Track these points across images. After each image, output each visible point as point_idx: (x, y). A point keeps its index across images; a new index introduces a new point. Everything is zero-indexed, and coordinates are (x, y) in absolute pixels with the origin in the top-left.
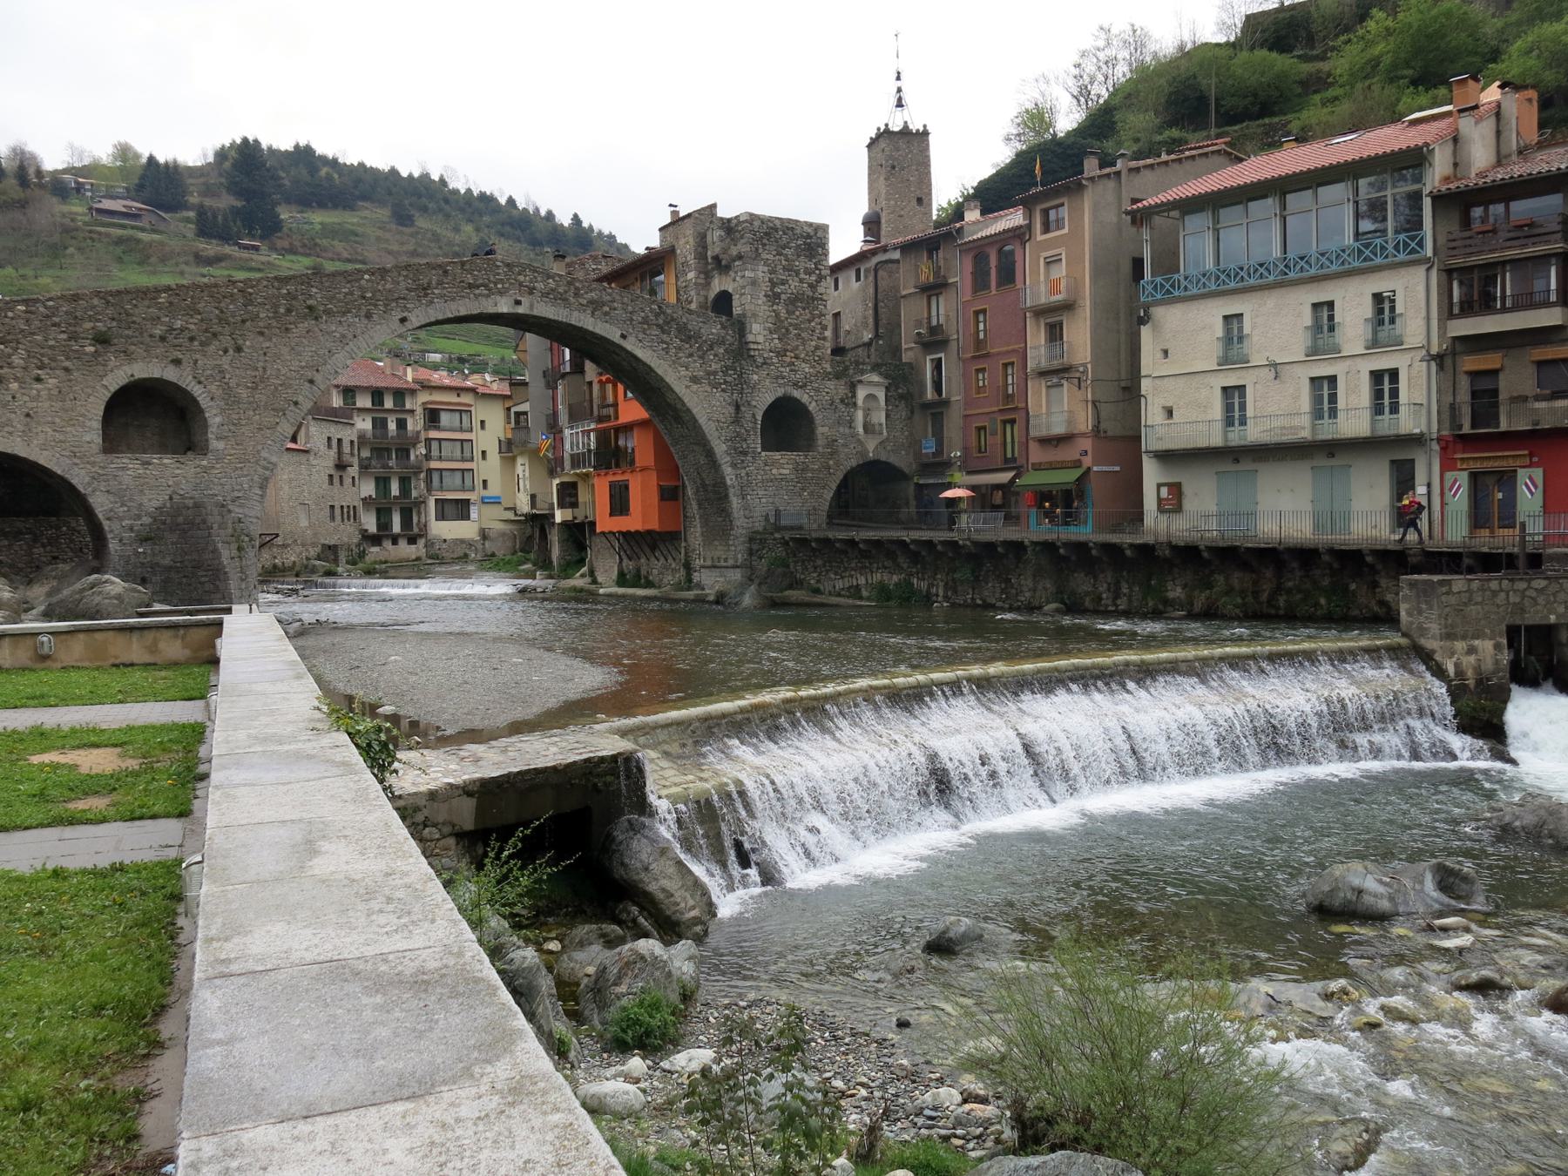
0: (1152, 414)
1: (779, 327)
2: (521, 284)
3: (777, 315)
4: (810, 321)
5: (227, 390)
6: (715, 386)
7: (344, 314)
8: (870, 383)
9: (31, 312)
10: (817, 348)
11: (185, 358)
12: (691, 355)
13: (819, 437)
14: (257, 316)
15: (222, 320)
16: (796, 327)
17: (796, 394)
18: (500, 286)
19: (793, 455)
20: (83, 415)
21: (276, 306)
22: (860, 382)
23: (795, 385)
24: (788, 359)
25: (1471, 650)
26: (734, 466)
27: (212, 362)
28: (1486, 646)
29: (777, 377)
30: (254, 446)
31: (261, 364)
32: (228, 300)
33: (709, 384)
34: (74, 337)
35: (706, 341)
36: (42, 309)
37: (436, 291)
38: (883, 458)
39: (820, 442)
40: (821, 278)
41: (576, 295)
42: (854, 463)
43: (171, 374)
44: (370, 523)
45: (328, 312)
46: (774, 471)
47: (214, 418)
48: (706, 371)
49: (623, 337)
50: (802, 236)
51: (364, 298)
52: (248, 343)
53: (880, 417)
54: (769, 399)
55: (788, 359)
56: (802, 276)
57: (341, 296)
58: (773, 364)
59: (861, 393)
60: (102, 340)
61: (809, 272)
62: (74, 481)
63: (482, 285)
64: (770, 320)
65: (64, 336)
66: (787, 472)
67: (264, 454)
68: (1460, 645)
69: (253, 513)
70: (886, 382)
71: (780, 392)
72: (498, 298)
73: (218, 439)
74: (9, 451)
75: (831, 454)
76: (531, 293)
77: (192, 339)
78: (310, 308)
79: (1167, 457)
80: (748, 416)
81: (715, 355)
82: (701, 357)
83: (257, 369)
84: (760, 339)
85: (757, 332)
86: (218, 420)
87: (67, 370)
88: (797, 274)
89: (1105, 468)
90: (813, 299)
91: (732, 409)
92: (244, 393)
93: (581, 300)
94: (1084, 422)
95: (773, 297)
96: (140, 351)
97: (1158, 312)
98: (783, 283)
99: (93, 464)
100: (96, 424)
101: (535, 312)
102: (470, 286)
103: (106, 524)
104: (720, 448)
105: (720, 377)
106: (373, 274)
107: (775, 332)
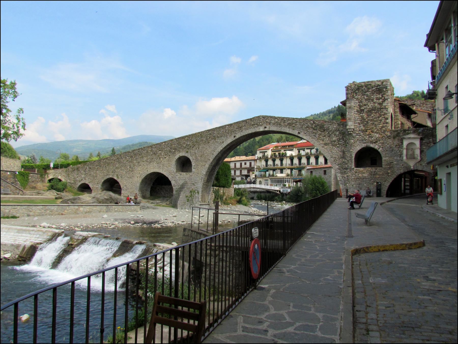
2: (267, 122)
3: (362, 117)
4: (379, 117)
5: (196, 157)
7: (221, 137)
8: (409, 138)
10: (382, 127)
11: (189, 151)
12: (325, 136)
13: (383, 161)
15: (196, 142)
16: (371, 120)
17: (372, 146)
19: (369, 169)
22: (404, 138)
23: (372, 142)
24: (367, 133)
26: (341, 173)
27: (193, 151)
29: (362, 140)
33: (332, 145)
35: (331, 131)
39: (383, 164)
40: (385, 100)
41: (284, 122)
42: (402, 171)
43: (186, 155)
45: (218, 137)
46: (359, 175)
47: (193, 164)
49: (299, 133)
50: (374, 85)
51: (226, 132)
53: (418, 152)
54: (358, 148)
55: (367, 133)
56: (374, 101)
58: (361, 135)
59: (405, 143)
61: (378, 99)
62: (169, 178)
64: (358, 120)
66: (367, 175)
67: (202, 172)
69: (200, 186)
71: (364, 145)
72: (260, 127)
73: (194, 169)
74: (160, 172)
75: (390, 168)
76: (270, 124)
77: (190, 147)
78: (214, 136)
80: (349, 156)
81: (335, 135)
82: (329, 136)
84: (353, 127)
85: (351, 125)
86: (194, 164)
87: (169, 155)
88: (372, 100)
90: (381, 109)
91: (341, 153)
92: (199, 158)
95: (361, 111)
96: (181, 150)
98: (365, 105)
99: (172, 174)
101: (271, 129)
102: (253, 125)
103: (173, 187)
107: (362, 124)
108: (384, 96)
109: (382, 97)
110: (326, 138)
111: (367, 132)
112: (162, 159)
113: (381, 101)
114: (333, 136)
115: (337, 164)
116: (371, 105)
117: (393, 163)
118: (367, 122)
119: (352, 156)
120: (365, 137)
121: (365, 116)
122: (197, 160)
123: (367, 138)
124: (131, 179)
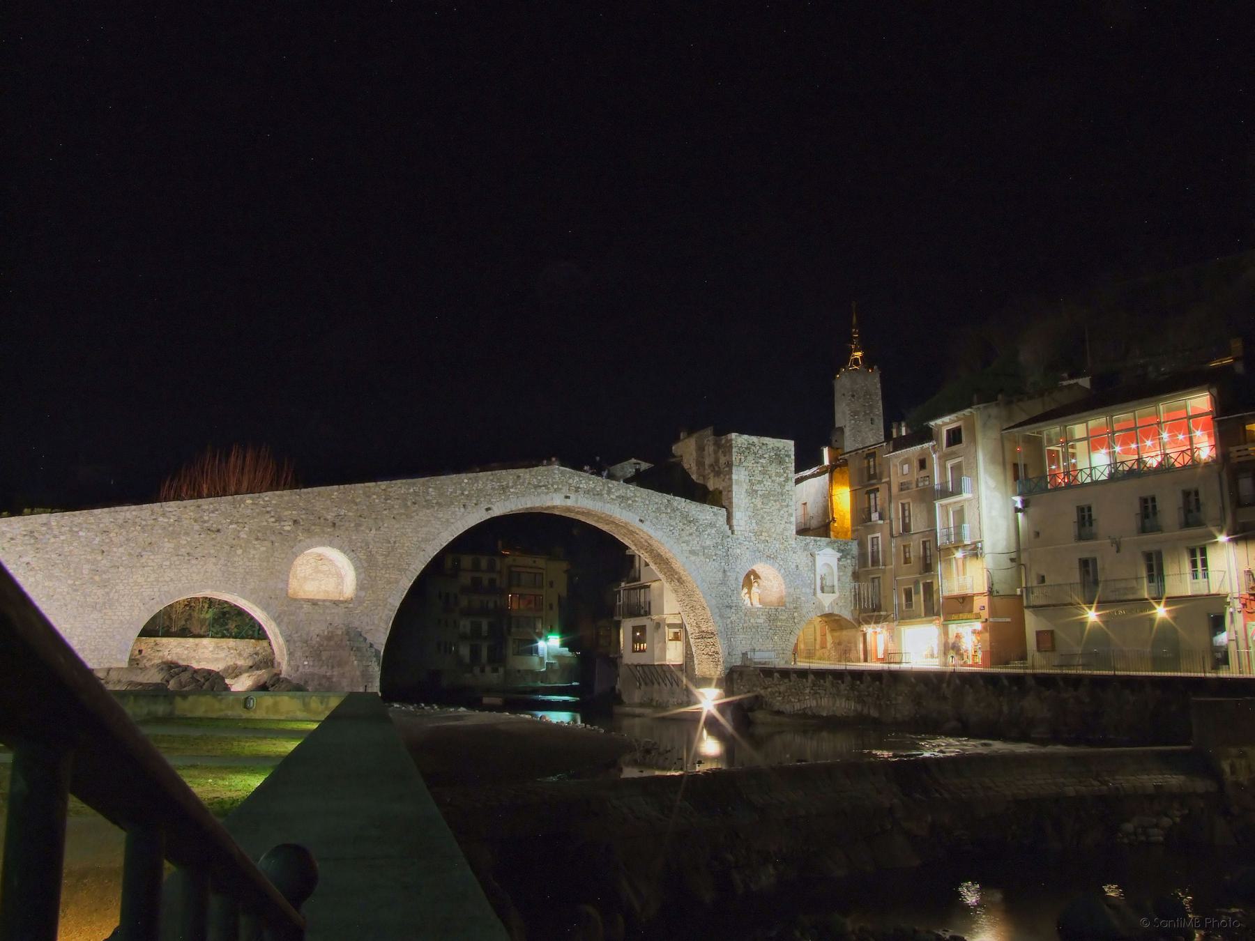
4: (779, 510)
6: (709, 557)
9: (255, 504)
10: (785, 529)
12: (691, 534)
14: (393, 507)
18: (555, 486)
20: (279, 572)
21: (405, 500)
30: (384, 595)
31: (393, 539)
32: (375, 497)
34: (279, 520)
35: (701, 525)
36: (261, 502)
37: (512, 490)
38: (836, 612)
48: (701, 546)
52: (386, 525)
55: (763, 538)
57: (449, 493)
60: (295, 522)
63: (543, 486)
65: (273, 520)
66: (762, 621)
67: (390, 600)
68: (1233, 751)
70: (839, 555)
75: (795, 608)
82: (697, 536)
83: (389, 542)
89: (1000, 620)
91: (720, 575)
92: (380, 559)
93: (612, 496)
96: (317, 529)
98: (760, 482)
105: (712, 551)
106: (470, 479)
108: (787, 471)
109: (785, 472)
110: (693, 540)
111: (761, 535)
112: (239, 552)
113: (782, 479)
114: (706, 536)
115: (713, 595)
117: (800, 598)
118: (763, 517)
119: (738, 581)
120: (759, 545)
121: (758, 502)
123: (761, 547)
124: (95, 615)
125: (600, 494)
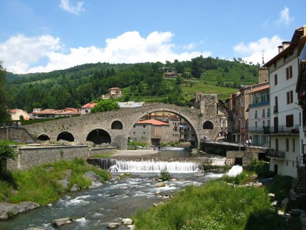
0: (249, 126)
1: (207, 110)
17: (210, 120)
25: (230, 160)
28: (232, 160)
40: (215, 102)
43: (119, 120)
44: (183, 137)
47: (124, 125)
54: (205, 121)
60: (112, 117)
79: (251, 132)
94: (245, 127)
95: (206, 106)
97: (250, 109)
100: (111, 126)
104: (195, 129)
116: (210, 104)
122: (125, 123)
125: (170, 108)
